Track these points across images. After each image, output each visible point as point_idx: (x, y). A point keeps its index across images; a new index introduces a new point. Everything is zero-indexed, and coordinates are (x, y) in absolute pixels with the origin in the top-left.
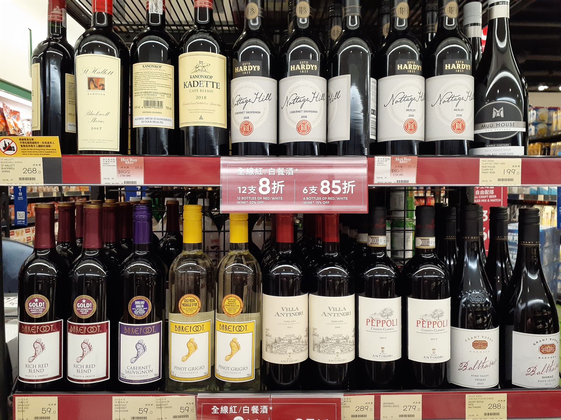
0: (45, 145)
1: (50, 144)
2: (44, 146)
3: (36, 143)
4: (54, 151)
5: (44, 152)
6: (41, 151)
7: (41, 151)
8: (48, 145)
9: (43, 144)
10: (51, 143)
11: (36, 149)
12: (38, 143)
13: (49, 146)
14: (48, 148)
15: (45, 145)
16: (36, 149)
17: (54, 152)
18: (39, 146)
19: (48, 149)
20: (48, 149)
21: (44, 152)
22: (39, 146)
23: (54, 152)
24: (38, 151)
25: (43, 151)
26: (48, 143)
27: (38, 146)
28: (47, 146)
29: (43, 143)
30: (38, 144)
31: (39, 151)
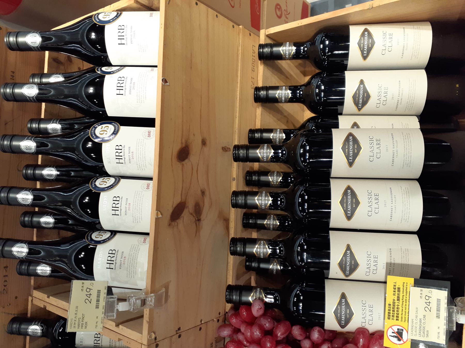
0: (397, 293)
1: (397, 287)
2: (398, 294)
3: (394, 303)
4: (405, 284)
5: (406, 297)
6: (404, 300)
7: (404, 300)
8: (397, 290)
9: (396, 295)
10: (395, 286)
11: (402, 305)
12: (394, 300)
13: (399, 288)
14: (401, 290)
15: (397, 293)
16: (402, 305)
17: (407, 285)
18: (398, 300)
19: (403, 292)
20: (403, 292)
21: (406, 297)
22: (398, 300)
23: (407, 285)
24: (404, 303)
25: (404, 297)
26: (395, 289)
27: (398, 302)
28: (398, 291)
29: (394, 295)
30: (396, 301)
31: (405, 301)
